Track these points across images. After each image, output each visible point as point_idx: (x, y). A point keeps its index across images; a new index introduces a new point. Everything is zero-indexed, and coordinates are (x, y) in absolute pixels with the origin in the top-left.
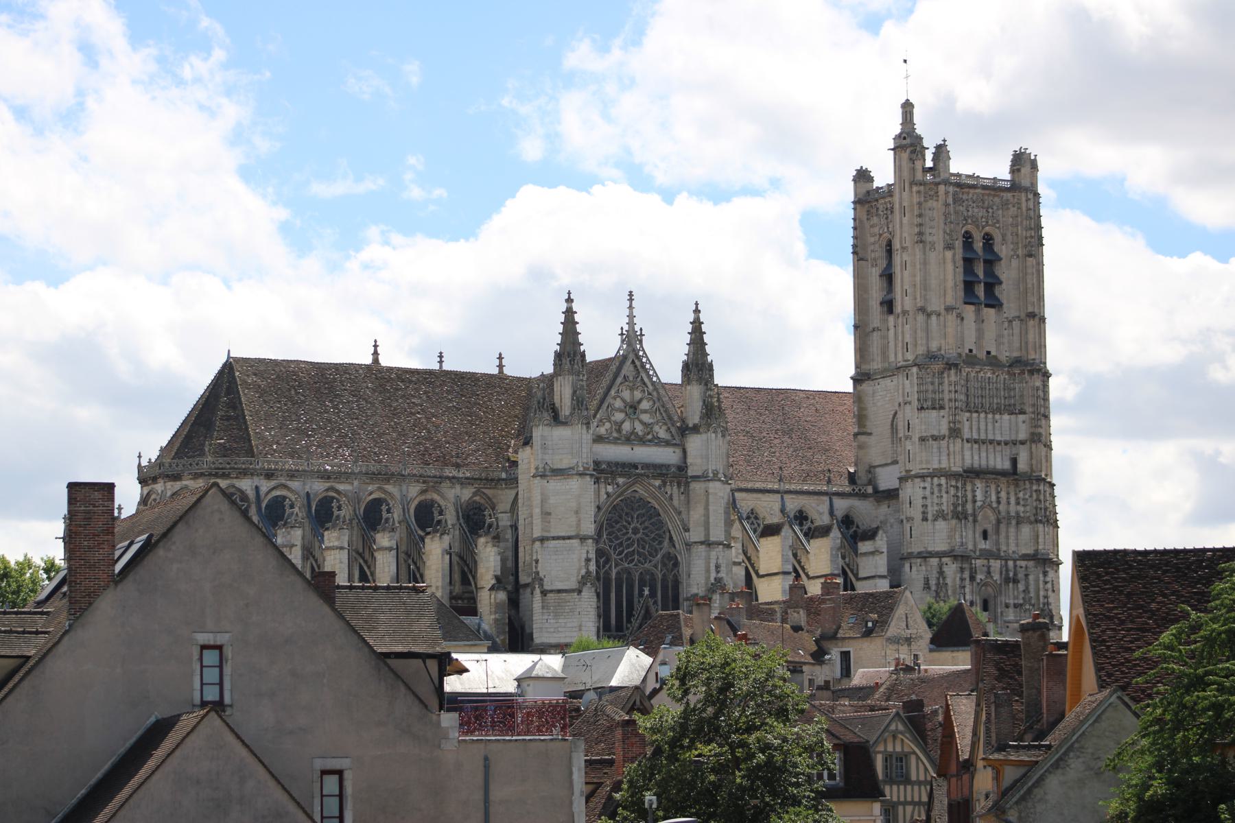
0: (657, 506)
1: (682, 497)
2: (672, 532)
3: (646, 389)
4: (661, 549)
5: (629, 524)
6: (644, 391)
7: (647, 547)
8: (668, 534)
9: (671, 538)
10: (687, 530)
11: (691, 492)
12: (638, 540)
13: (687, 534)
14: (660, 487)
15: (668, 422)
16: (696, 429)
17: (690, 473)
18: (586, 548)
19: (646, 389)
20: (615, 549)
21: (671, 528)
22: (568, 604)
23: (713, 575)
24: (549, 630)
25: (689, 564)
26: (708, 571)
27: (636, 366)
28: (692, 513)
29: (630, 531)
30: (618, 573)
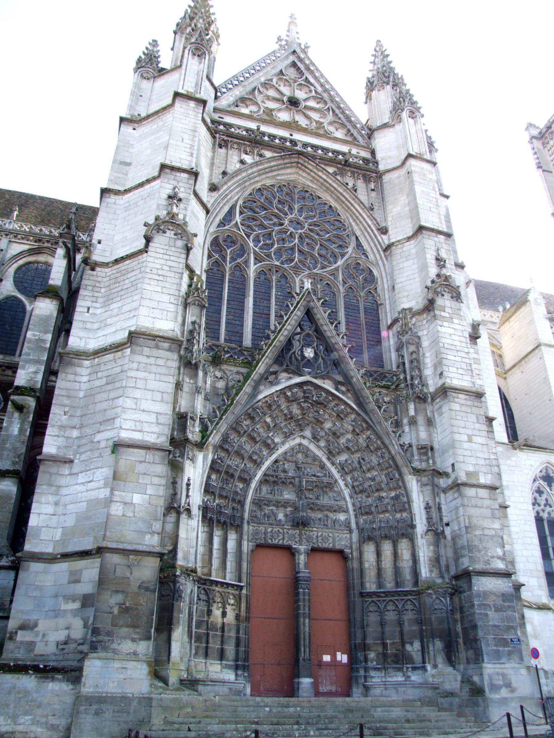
0: (334, 204)
1: (373, 194)
2: (362, 239)
3: (312, 88)
4: (343, 255)
5: (286, 214)
6: (311, 91)
7: (317, 248)
8: (353, 238)
9: (359, 245)
10: (384, 231)
11: (385, 186)
12: (301, 237)
13: (384, 237)
14: (335, 174)
15: (348, 124)
16: (385, 126)
17: (382, 167)
18: (175, 183)
19: (312, 88)
20: (257, 240)
21: (358, 233)
22: (130, 275)
23: (433, 271)
24: (89, 326)
25: (392, 272)
26: (424, 268)
27: (298, 69)
28: (389, 207)
29: (286, 222)
30: (260, 273)
